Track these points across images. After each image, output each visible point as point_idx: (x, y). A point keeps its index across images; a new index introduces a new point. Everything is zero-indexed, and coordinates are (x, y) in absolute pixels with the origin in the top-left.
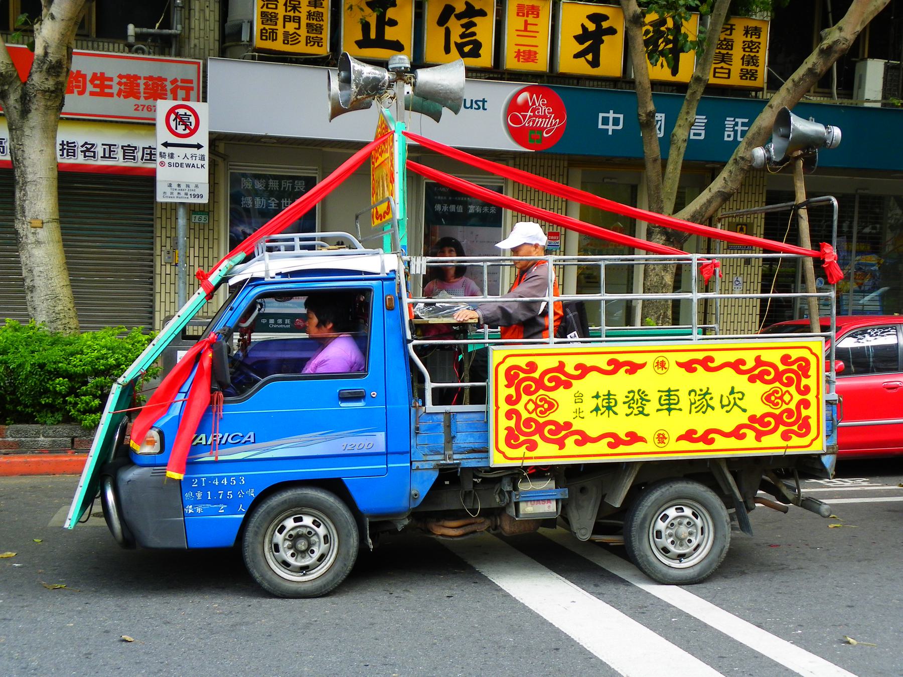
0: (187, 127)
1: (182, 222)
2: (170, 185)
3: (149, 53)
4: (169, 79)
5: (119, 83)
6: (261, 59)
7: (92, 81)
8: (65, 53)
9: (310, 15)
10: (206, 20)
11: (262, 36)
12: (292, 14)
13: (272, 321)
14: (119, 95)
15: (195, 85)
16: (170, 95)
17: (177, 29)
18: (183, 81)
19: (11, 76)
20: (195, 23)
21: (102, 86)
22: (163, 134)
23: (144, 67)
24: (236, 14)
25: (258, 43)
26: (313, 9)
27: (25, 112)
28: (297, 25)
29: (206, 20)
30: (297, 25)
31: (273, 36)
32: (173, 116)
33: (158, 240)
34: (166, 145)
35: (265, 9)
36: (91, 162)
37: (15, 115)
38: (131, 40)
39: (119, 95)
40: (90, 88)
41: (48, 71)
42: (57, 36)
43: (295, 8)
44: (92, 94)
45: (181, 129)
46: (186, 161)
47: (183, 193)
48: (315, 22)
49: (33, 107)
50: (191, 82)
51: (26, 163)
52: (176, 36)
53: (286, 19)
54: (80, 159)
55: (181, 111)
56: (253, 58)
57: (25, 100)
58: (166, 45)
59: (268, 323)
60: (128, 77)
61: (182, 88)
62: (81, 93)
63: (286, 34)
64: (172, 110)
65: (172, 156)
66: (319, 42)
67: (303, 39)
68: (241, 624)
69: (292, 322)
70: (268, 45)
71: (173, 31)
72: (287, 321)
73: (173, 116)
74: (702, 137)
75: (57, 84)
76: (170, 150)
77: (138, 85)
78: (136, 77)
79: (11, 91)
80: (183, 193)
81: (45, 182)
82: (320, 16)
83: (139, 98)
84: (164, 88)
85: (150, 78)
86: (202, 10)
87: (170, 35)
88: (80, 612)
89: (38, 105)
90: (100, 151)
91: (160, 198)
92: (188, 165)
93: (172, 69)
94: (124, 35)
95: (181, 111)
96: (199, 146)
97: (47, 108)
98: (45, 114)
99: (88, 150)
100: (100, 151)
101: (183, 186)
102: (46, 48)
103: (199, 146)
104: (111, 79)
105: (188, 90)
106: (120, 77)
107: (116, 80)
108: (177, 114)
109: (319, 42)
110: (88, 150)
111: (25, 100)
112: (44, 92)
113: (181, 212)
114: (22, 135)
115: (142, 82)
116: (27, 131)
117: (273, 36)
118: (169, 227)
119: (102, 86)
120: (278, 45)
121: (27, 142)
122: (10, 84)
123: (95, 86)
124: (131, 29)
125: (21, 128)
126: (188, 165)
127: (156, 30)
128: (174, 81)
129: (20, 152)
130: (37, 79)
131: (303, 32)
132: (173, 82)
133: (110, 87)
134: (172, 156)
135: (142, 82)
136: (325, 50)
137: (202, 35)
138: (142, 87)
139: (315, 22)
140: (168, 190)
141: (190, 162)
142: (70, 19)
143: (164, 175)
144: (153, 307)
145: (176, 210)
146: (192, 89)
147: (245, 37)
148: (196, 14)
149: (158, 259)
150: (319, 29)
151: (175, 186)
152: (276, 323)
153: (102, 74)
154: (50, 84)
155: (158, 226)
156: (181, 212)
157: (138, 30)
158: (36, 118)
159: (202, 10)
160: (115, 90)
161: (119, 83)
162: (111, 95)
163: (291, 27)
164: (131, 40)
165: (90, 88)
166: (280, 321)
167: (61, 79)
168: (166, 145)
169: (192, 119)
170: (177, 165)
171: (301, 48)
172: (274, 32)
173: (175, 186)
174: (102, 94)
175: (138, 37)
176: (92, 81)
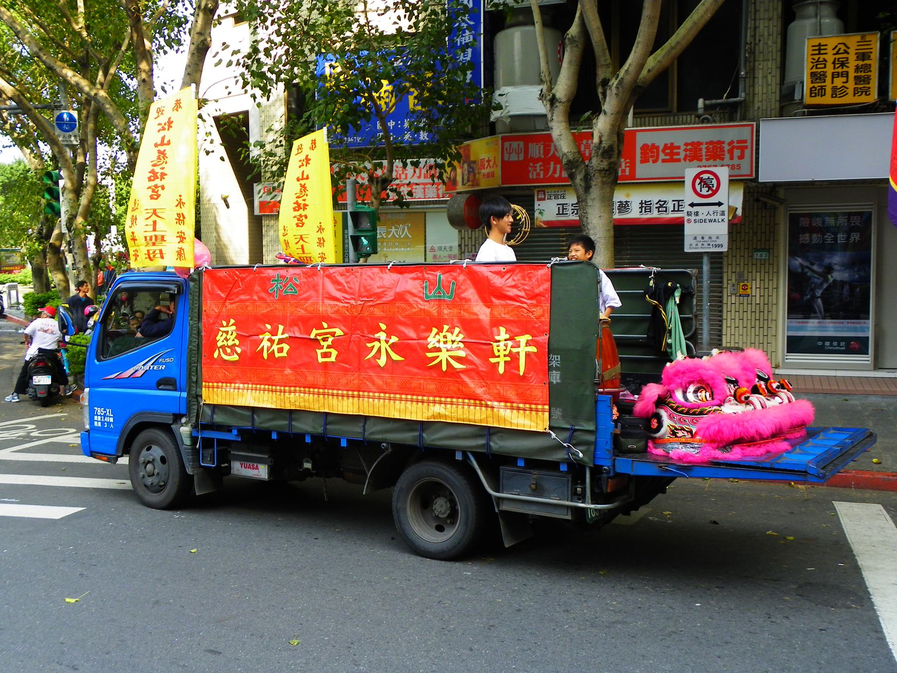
0: (710, 188)
1: (706, 268)
2: (695, 238)
3: (714, 121)
4: (728, 141)
5: (685, 150)
6: (811, 114)
7: (663, 151)
8: (616, 139)
9: (857, 69)
10: (768, 85)
11: (811, 93)
12: (840, 70)
13: (827, 344)
14: (685, 159)
15: (749, 144)
16: (727, 156)
17: (742, 96)
18: (738, 142)
19: (577, 161)
20: (758, 89)
21: (672, 154)
22: (688, 195)
23: (704, 134)
24: (791, 77)
25: (808, 100)
26: (860, 63)
27: (587, 188)
28: (844, 79)
29: (768, 85)
30: (844, 79)
31: (822, 92)
32: (698, 181)
33: (725, 275)
34: (692, 205)
35: (814, 70)
36: (664, 216)
37: (581, 191)
38: (701, 111)
39: (685, 159)
40: (662, 156)
41: (603, 154)
42: (608, 127)
43: (843, 65)
44: (664, 161)
45: (704, 191)
46: (709, 217)
47: (706, 244)
48: (863, 74)
49: (593, 183)
50: (745, 141)
51: (589, 227)
52: (740, 102)
53: (834, 76)
54: (655, 214)
55: (705, 176)
56: (803, 114)
57: (587, 179)
58: (733, 112)
59: (824, 345)
60: (692, 144)
61: (738, 148)
62: (654, 162)
63: (834, 89)
64: (697, 176)
65: (697, 214)
66: (867, 92)
67: (850, 91)
68: (620, 623)
69: (848, 345)
70: (818, 100)
71: (738, 99)
72: (842, 344)
73: (698, 181)
74: (333, 359)
75: (610, 164)
76: (696, 209)
77: (701, 150)
78: (700, 143)
79: (577, 173)
80: (706, 244)
81: (602, 241)
82: (867, 68)
83: (701, 160)
84: (722, 150)
85: (711, 143)
86: (765, 77)
87: (737, 103)
88: (514, 591)
89: (596, 182)
90: (670, 206)
91: (687, 249)
92: (710, 221)
93: (731, 133)
94: (696, 108)
95: (705, 176)
96: (720, 204)
97: (603, 183)
98: (602, 188)
99: (661, 206)
100: (670, 206)
101: (706, 239)
102: (600, 137)
103: (720, 204)
104: (679, 148)
105: (743, 149)
106: (686, 144)
107: (683, 147)
108: (702, 180)
109: (867, 92)
110: (661, 206)
111: (587, 179)
112: (600, 171)
113: (705, 260)
114: (586, 205)
115: (704, 147)
116: (590, 203)
117: (822, 92)
118: (734, 263)
119: (672, 154)
120: (827, 100)
121: (589, 210)
122: (577, 168)
123: (666, 154)
124: (701, 103)
125: (585, 201)
126: (710, 221)
127: (724, 100)
128: (732, 142)
129: (585, 219)
130: (595, 161)
131: (851, 85)
132: (730, 144)
133: (678, 154)
134: (697, 214)
135: (704, 147)
136: (873, 97)
137: (765, 98)
138: (704, 150)
139: (863, 74)
140: (694, 242)
141: (712, 217)
142: (618, 113)
143: (690, 230)
144: (721, 331)
145: (702, 258)
146: (746, 147)
147: (797, 97)
148: (760, 81)
149: (725, 291)
150: (867, 80)
151: (699, 238)
152: (831, 345)
153: (672, 144)
154: (605, 164)
155: (725, 263)
156: (705, 260)
157: (708, 102)
158: (595, 192)
159: (765, 77)
160: (682, 156)
161: (685, 150)
162: (679, 160)
163: (839, 82)
164: (701, 111)
165: (662, 156)
166: (835, 343)
167: (613, 159)
168: (692, 205)
169: (714, 182)
170: (701, 221)
171: (849, 99)
172: (822, 88)
173: (699, 238)
174: (672, 160)
175: (706, 107)
176: (663, 151)
